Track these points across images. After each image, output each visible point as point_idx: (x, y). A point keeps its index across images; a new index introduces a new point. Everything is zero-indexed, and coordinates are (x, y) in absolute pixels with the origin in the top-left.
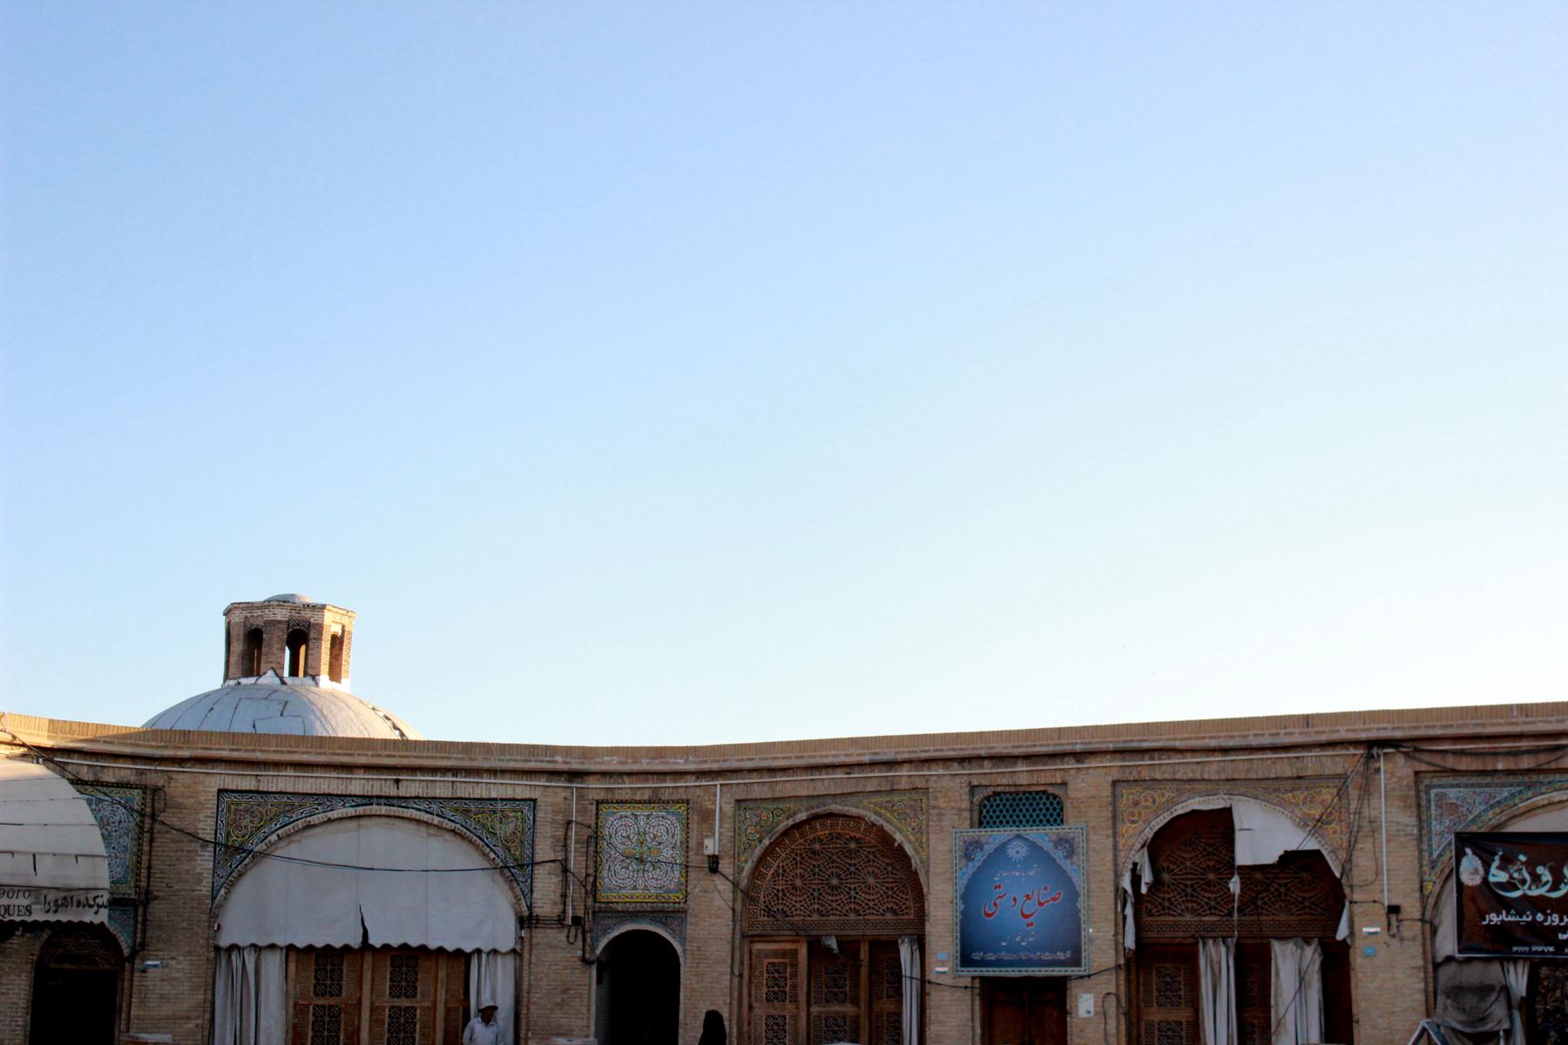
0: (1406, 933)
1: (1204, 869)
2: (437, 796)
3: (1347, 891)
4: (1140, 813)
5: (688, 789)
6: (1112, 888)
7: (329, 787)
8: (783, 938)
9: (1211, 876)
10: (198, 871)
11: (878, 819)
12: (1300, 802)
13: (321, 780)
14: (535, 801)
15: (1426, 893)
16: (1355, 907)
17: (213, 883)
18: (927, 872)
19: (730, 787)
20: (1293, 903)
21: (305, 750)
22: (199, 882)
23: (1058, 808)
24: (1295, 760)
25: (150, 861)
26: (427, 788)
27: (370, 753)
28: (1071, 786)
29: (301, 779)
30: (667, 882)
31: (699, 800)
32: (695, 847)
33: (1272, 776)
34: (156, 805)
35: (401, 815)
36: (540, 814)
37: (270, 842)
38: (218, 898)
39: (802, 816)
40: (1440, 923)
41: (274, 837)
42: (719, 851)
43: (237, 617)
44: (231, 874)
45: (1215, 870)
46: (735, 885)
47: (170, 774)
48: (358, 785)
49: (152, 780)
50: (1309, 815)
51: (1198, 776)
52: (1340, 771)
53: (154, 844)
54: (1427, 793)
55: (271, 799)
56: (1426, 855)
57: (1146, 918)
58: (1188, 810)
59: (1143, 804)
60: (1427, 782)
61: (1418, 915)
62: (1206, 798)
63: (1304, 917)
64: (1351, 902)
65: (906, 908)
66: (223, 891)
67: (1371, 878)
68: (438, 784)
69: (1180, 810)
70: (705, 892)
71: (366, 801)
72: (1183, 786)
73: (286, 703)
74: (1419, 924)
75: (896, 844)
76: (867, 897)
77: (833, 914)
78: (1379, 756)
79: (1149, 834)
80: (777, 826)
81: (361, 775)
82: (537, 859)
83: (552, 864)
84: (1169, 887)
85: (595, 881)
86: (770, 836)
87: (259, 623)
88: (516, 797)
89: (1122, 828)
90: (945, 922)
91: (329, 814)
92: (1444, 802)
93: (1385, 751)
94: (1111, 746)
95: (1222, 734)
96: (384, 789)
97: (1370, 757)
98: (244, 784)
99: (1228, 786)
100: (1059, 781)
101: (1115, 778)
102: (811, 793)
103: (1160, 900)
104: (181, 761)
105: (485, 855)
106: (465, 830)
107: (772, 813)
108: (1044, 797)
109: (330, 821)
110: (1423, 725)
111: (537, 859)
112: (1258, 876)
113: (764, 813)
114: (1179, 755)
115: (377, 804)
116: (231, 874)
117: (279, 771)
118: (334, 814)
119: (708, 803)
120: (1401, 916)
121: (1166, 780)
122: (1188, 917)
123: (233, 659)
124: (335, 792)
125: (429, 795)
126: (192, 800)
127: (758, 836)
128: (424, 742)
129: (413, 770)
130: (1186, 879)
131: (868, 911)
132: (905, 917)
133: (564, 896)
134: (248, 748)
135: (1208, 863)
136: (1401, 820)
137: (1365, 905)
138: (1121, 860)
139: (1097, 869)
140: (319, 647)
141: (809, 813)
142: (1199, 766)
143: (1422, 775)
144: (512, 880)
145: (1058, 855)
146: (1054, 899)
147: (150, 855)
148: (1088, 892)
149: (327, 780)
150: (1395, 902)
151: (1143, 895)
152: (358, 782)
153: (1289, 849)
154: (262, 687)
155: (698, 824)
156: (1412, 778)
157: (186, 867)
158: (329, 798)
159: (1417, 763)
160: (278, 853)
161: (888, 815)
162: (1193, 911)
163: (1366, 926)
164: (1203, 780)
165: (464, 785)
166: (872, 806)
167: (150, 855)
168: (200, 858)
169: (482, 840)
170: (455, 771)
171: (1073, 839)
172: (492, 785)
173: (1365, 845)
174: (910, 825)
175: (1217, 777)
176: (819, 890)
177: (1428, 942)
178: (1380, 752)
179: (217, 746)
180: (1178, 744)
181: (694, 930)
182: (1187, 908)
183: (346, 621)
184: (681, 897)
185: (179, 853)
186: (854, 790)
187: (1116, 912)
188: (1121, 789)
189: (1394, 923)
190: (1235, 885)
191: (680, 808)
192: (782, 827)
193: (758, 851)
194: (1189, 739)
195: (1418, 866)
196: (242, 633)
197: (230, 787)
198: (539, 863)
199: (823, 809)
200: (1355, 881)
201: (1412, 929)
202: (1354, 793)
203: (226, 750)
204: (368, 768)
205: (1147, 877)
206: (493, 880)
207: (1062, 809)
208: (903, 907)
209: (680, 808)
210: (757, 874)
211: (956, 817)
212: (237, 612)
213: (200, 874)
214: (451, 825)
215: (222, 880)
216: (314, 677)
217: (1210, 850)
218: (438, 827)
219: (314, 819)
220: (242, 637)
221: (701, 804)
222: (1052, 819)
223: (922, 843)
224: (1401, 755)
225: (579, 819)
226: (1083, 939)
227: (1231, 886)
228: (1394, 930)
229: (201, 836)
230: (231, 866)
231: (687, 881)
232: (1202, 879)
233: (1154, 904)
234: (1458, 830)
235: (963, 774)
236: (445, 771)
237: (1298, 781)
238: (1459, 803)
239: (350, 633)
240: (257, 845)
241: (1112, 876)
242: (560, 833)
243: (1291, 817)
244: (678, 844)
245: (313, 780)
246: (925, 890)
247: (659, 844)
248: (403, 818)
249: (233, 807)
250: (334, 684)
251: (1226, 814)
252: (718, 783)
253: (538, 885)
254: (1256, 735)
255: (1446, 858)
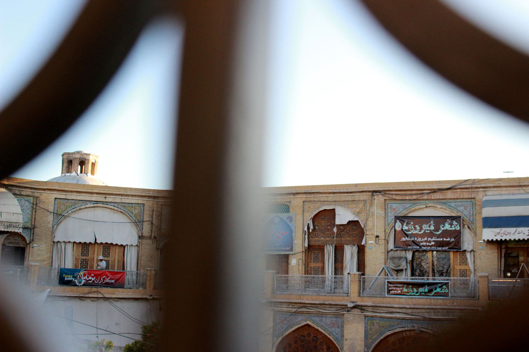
0: (380, 243)
1: (327, 225)
2: (117, 202)
3: (365, 231)
4: (310, 210)
6: (302, 230)
7: (86, 198)
9: (329, 227)
10: (49, 220)
12: (354, 207)
13: (84, 196)
14: (144, 204)
15: (386, 232)
16: (367, 236)
17: (53, 224)
20: (351, 235)
21: (79, 188)
22: (49, 223)
23: (288, 208)
24: (352, 196)
25: (35, 217)
26: (114, 199)
27: (98, 189)
28: (292, 202)
29: (78, 196)
33: (346, 200)
34: (37, 202)
35: (106, 207)
36: (145, 208)
37: (69, 213)
38: (54, 228)
40: (390, 240)
41: (70, 212)
43: (65, 157)
44: (58, 221)
45: (330, 226)
47: (41, 193)
48: (95, 198)
49: (36, 194)
50: (356, 211)
51: (326, 200)
52: (364, 199)
53: (36, 212)
54: (388, 205)
55: (70, 201)
56: (387, 222)
57: (311, 239)
58: (323, 209)
59: (311, 207)
60: (388, 202)
61: (384, 238)
62: (328, 206)
63: (353, 239)
64: (366, 235)
66: (56, 226)
67: (371, 228)
68: (117, 198)
69: (321, 209)
71: (97, 203)
72: (322, 203)
73: (78, 180)
74: (384, 240)
78: (375, 195)
79: (313, 216)
81: (95, 195)
82: (144, 220)
83: (148, 222)
84: (317, 230)
85: (160, 227)
87: (71, 158)
88: (139, 203)
89: (305, 214)
91: (86, 206)
92: (392, 208)
93: (377, 194)
94: (303, 192)
95: (333, 189)
96: (102, 199)
97: (373, 195)
98: (62, 197)
99: (334, 203)
100: (289, 201)
101: (304, 200)
103: (315, 234)
104: (45, 190)
105: (130, 219)
106: (124, 212)
108: (284, 205)
109: (86, 208)
110: (387, 187)
111: (144, 220)
112: (342, 227)
114: (322, 194)
115: (100, 204)
116: (58, 221)
117: (72, 193)
118: (88, 206)
120: (379, 238)
121: (318, 201)
122: (322, 238)
123: (64, 169)
124: (88, 200)
125: (114, 202)
126: (47, 201)
128: (113, 187)
129: (110, 194)
130: (322, 228)
133: (151, 231)
134: (63, 187)
135: (328, 224)
136: (380, 213)
137: (370, 235)
138: (304, 223)
139: (298, 225)
140: (88, 165)
142: (327, 197)
143: (386, 200)
144: (137, 226)
145: (288, 221)
146: (286, 233)
147: (35, 215)
148: (295, 231)
149: (86, 196)
150: (378, 235)
151: (310, 232)
152: (94, 197)
153: (350, 220)
154: (72, 176)
156: (384, 201)
157: (45, 219)
158: (86, 201)
159: (385, 197)
160: (71, 216)
162: (323, 237)
163: (370, 241)
164: (328, 201)
165: (124, 199)
167: (35, 215)
168: (49, 217)
169: (129, 215)
170: (122, 195)
171: (292, 217)
172: (132, 200)
173: (370, 219)
175: (331, 200)
177: (386, 245)
178: (375, 194)
179: (55, 186)
180: (321, 191)
182: (322, 236)
183: (96, 158)
185: (43, 215)
187: (303, 237)
188: (306, 203)
189: (377, 240)
190: (335, 230)
194: (324, 190)
195: (384, 225)
196: (66, 161)
197: (58, 198)
198: (144, 221)
200: (367, 229)
201: (382, 242)
202: (368, 205)
203: (57, 187)
204: (97, 193)
205: (311, 227)
206: (132, 226)
207: (289, 209)
212: (65, 155)
213: (49, 221)
214: (120, 210)
215: (56, 223)
216: (86, 174)
217: (329, 220)
218: (116, 210)
219: (82, 207)
220: (66, 162)
222: (286, 212)
224: (381, 195)
225: (156, 210)
226: (294, 244)
227: (334, 230)
228: (377, 242)
229: (50, 211)
230: (58, 219)
232: (327, 228)
233: (313, 235)
234: (396, 215)
236: (119, 195)
237: (353, 202)
238: (396, 208)
239: (97, 162)
240: (65, 214)
241: (302, 227)
242: (151, 213)
243: (351, 212)
245: (82, 196)
248: (107, 208)
249: (59, 203)
250: (92, 176)
251: (334, 210)
253: (144, 227)
254: (342, 189)
255: (392, 223)
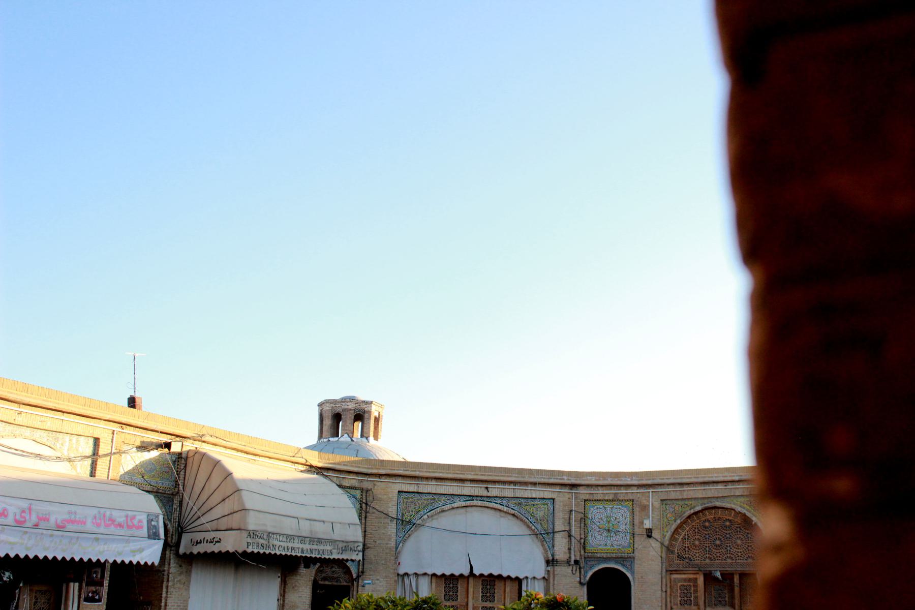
2: (507, 496)
7: (453, 491)
10: (389, 533)
11: (743, 510)
13: (450, 487)
14: (553, 499)
17: (396, 540)
21: (440, 471)
22: (390, 539)
25: (365, 528)
26: (501, 492)
27: (473, 473)
29: (439, 486)
34: (368, 499)
35: (488, 506)
36: (557, 506)
37: (424, 519)
38: (399, 548)
39: (699, 508)
41: (425, 517)
42: (652, 526)
43: (327, 407)
44: (405, 535)
46: (662, 544)
47: (375, 483)
48: (468, 490)
49: (366, 485)
53: (367, 519)
55: (424, 496)
66: (401, 544)
68: (507, 490)
71: (471, 498)
73: (358, 450)
76: (737, 550)
81: (468, 484)
82: (556, 530)
83: (563, 533)
85: (585, 541)
87: (339, 410)
88: (545, 497)
91: (453, 505)
96: (480, 492)
98: (411, 488)
102: (704, 496)
104: (380, 476)
105: (528, 527)
106: (519, 514)
107: (681, 506)
109: (453, 508)
111: (556, 530)
113: (677, 507)
115: (476, 500)
116: (405, 535)
117: (428, 482)
118: (455, 505)
119: (644, 501)
123: (325, 428)
124: (456, 493)
125: (502, 496)
126: (385, 496)
128: (499, 468)
129: (494, 482)
133: (570, 549)
134: (413, 469)
140: (369, 423)
144: (543, 542)
147: (365, 525)
149: (452, 487)
152: (467, 488)
154: (342, 443)
155: (639, 512)
157: (383, 532)
158: (453, 496)
160: (427, 524)
161: (748, 507)
165: (519, 491)
167: (365, 525)
168: (390, 527)
169: (528, 520)
170: (514, 483)
172: (533, 491)
176: (709, 547)
179: (397, 468)
183: (380, 410)
184: (631, 550)
185: (380, 524)
186: (729, 495)
191: (629, 504)
192: (687, 514)
193: (674, 527)
196: (330, 415)
197: (404, 490)
198: (556, 532)
203: (401, 470)
204: (472, 481)
206: (533, 540)
209: (629, 504)
212: (328, 405)
213: (389, 535)
214: (513, 512)
215: (401, 539)
216: (367, 438)
218: (506, 512)
219: (445, 508)
220: (330, 417)
225: (576, 509)
229: (390, 515)
230: (405, 531)
231: (634, 542)
236: (510, 483)
239: (382, 416)
240: (418, 520)
242: (567, 516)
245: (445, 487)
248: (488, 507)
249: (405, 500)
250: (376, 441)
253: (556, 543)
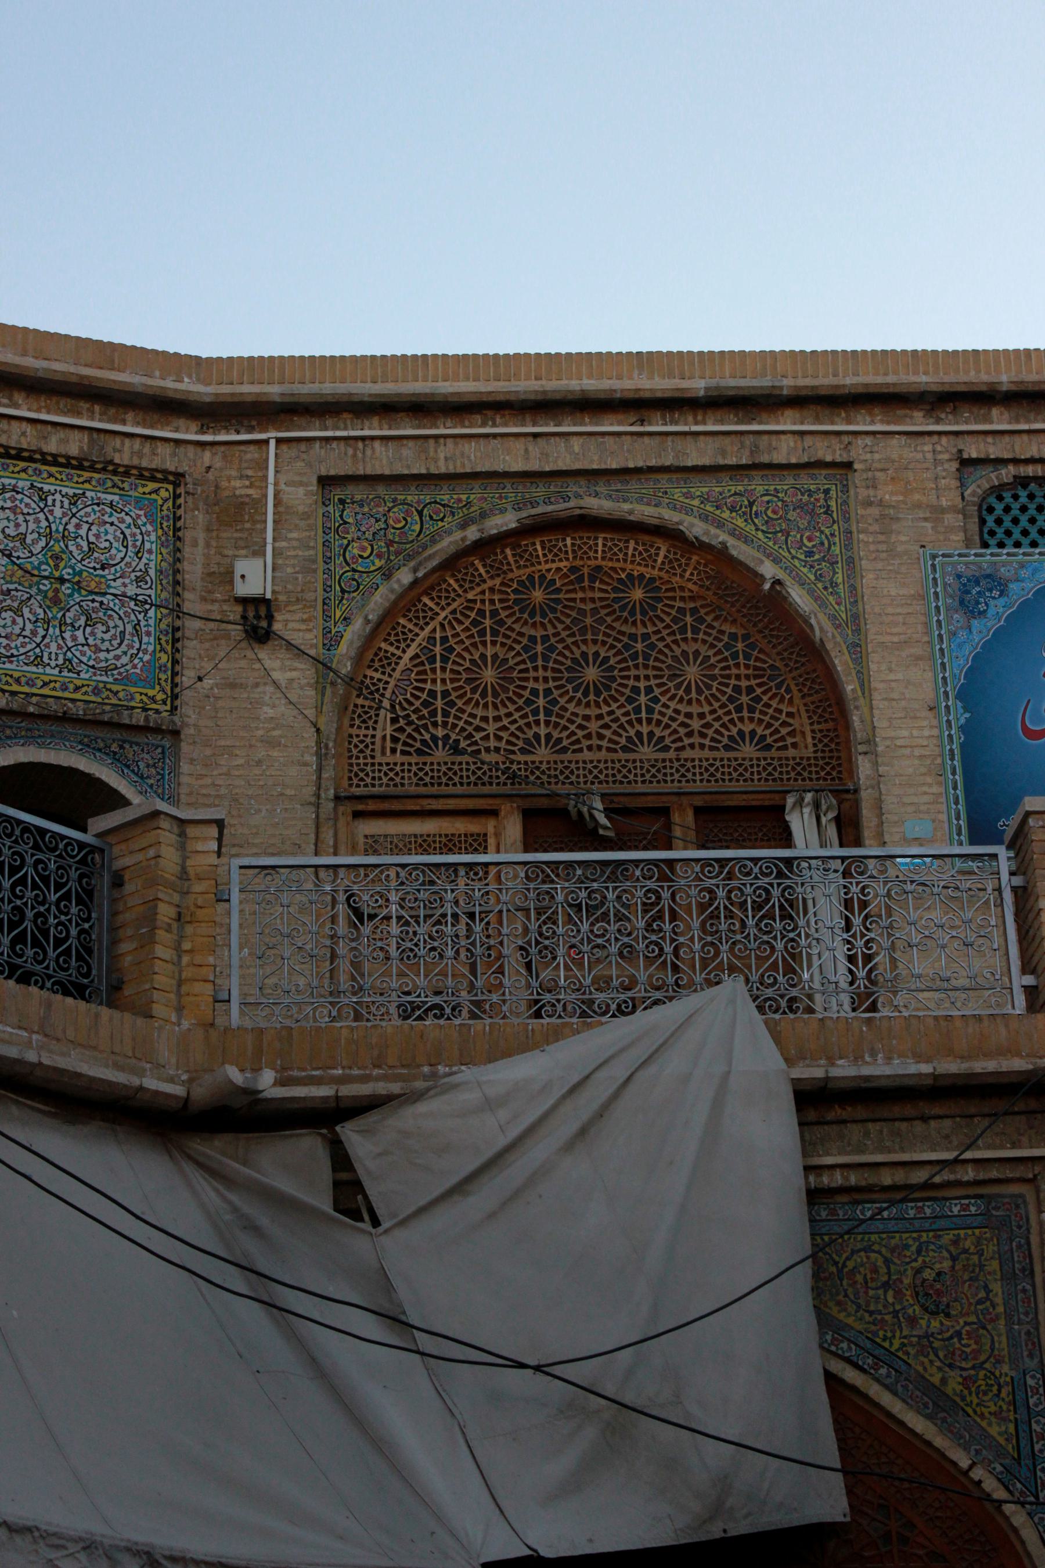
5: (182, 450)
8: (451, 804)
11: (713, 531)
18: (857, 650)
19: (303, 446)
30: (125, 660)
31: (210, 476)
32: (199, 585)
39: (506, 521)
42: (274, 592)
46: (323, 665)
65: (792, 734)
70: (233, 686)
75: (767, 586)
76: (683, 708)
77: (590, 748)
80: (434, 541)
86: (412, 564)
90: (917, 752)
102: (534, 466)
107: (420, 513)
113: (397, 513)
119: (237, 483)
127: (378, 563)
131: (687, 741)
132: (791, 752)
141: (524, 514)
155: (208, 530)
161: (740, 522)
166: (696, 502)
174: (801, 545)
176: (548, 692)
181: (201, 776)
184: (160, 696)
186: (653, 463)
191: (156, 491)
192: (448, 544)
193: (380, 599)
199: (563, 506)
208: (784, 731)
209: (156, 491)
210: (370, 655)
211: (928, 525)
221: (217, 487)
223: (834, 584)
231: (175, 662)
235: (940, 433)
244: (152, 572)
246: (850, 687)
247: (103, 568)
252: (272, 434)
